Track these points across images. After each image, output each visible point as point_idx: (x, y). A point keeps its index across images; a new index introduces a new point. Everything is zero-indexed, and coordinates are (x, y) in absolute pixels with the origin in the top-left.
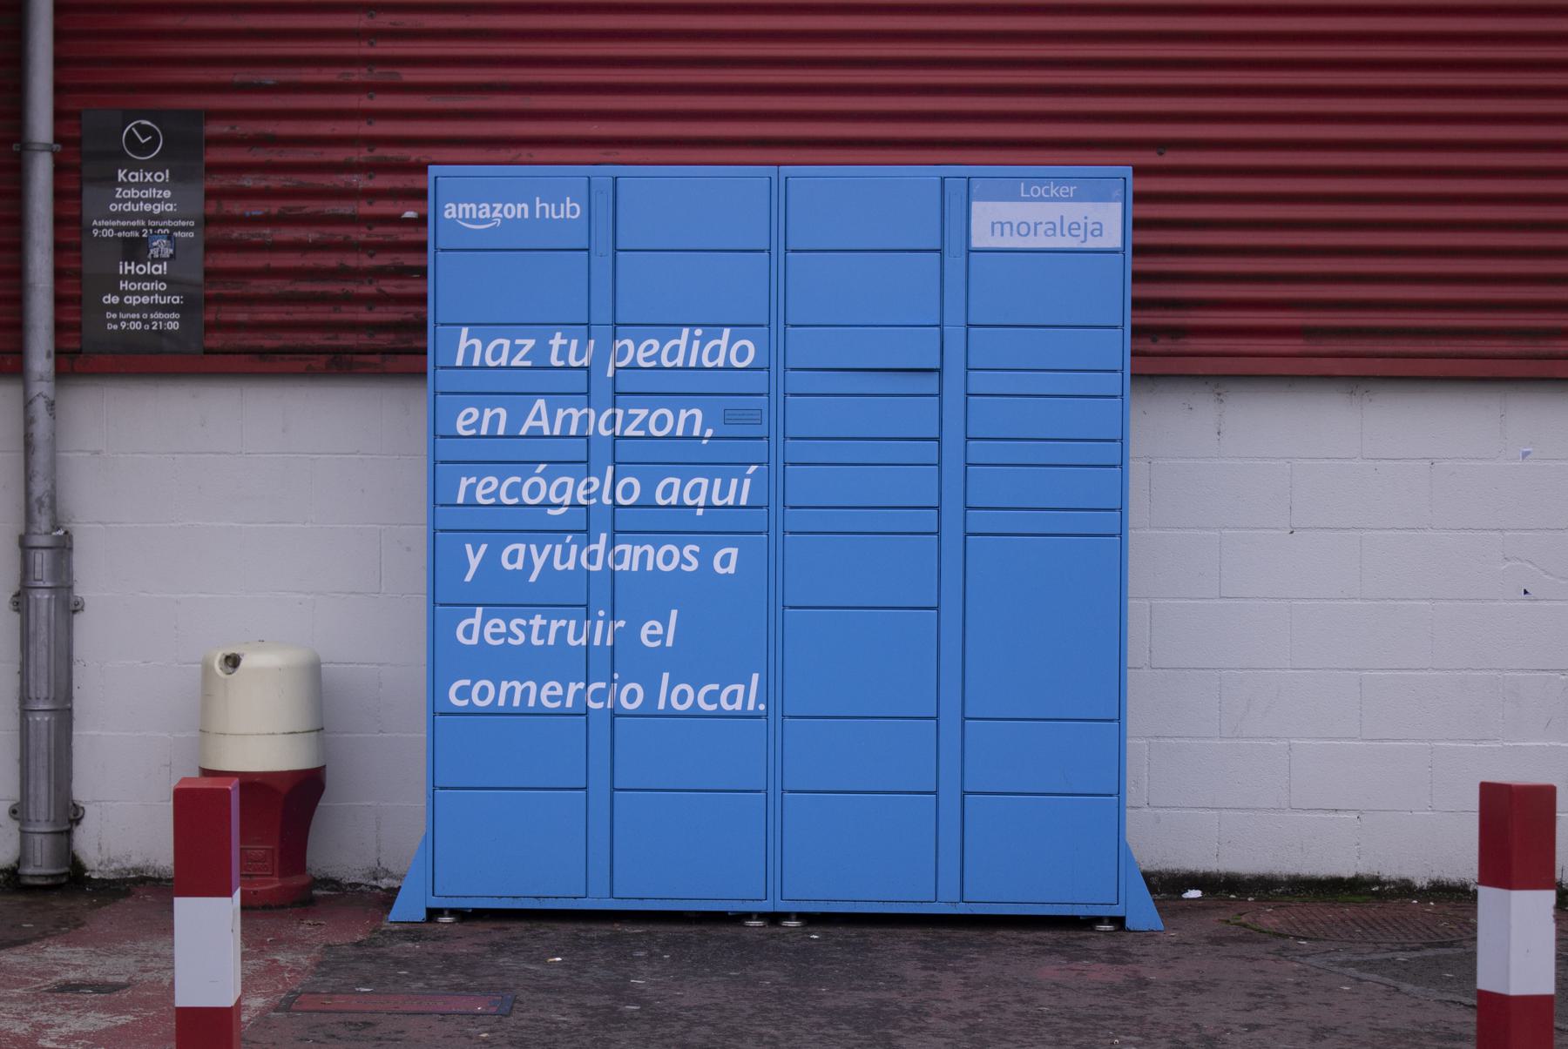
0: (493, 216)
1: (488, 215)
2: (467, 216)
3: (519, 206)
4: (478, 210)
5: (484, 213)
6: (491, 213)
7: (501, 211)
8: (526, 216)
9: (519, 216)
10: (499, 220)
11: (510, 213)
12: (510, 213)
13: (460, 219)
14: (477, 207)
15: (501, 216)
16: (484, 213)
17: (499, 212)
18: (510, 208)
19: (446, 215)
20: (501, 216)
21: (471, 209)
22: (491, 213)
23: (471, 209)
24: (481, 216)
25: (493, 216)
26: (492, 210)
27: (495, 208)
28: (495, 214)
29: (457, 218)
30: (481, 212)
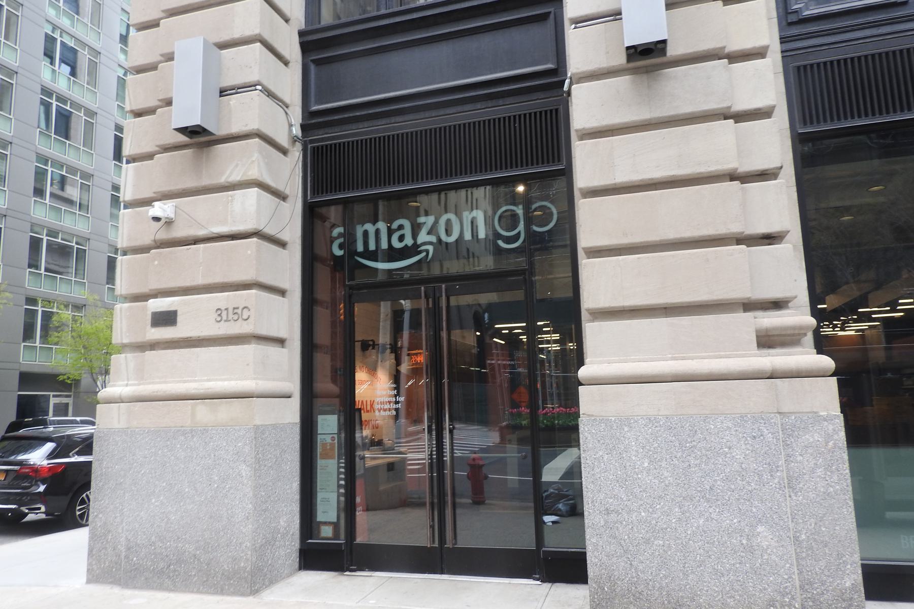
1: (409, 241)
2: (372, 247)
3: (467, 216)
4: (390, 232)
5: (401, 238)
6: (415, 236)
10: (430, 248)
12: (448, 232)
13: (361, 255)
15: (433, 239)
17: (428, 233)
20: (433, 239)
21: (377, 232)
22: (415, 236)
23: (377, 232)
24: (397, 244)
25: (420, 240)
26: (416, 229)
28: (423, 237)
30: (395, 238)
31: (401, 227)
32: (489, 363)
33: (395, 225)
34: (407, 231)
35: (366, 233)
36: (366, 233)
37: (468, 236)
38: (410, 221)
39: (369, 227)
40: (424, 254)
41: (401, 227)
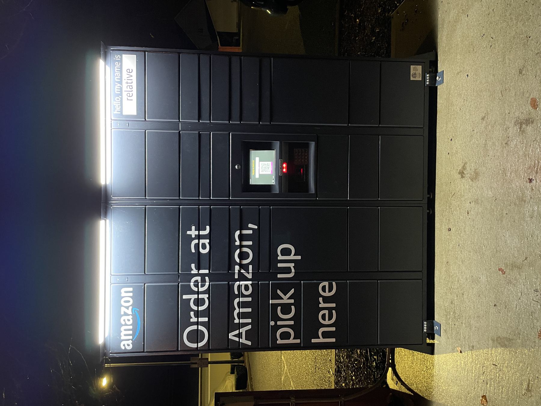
0: (131, 314)
1: (130, 317)
7: (127, 308)
8: (131, 289)
9: (131, 294)
11: (129, 302)
12: (129, 302)
14: (123, 325)
16: (129, 320)
18: (126, 302)
19: (129, 348)
20: (131, 308)
26: (126, 314)
27: (124, 312)
29: (132, 340)
30: (128, 323)
31: (124, 320)
32: (210, 360)
33: (123, 323)
34: (126, 318)
35: (125, 335)
36: (125, 335)
37: (131, 294)
38: (121, 290)
39: (122, 334)
40: (136, 311)
41: (124, 320)
